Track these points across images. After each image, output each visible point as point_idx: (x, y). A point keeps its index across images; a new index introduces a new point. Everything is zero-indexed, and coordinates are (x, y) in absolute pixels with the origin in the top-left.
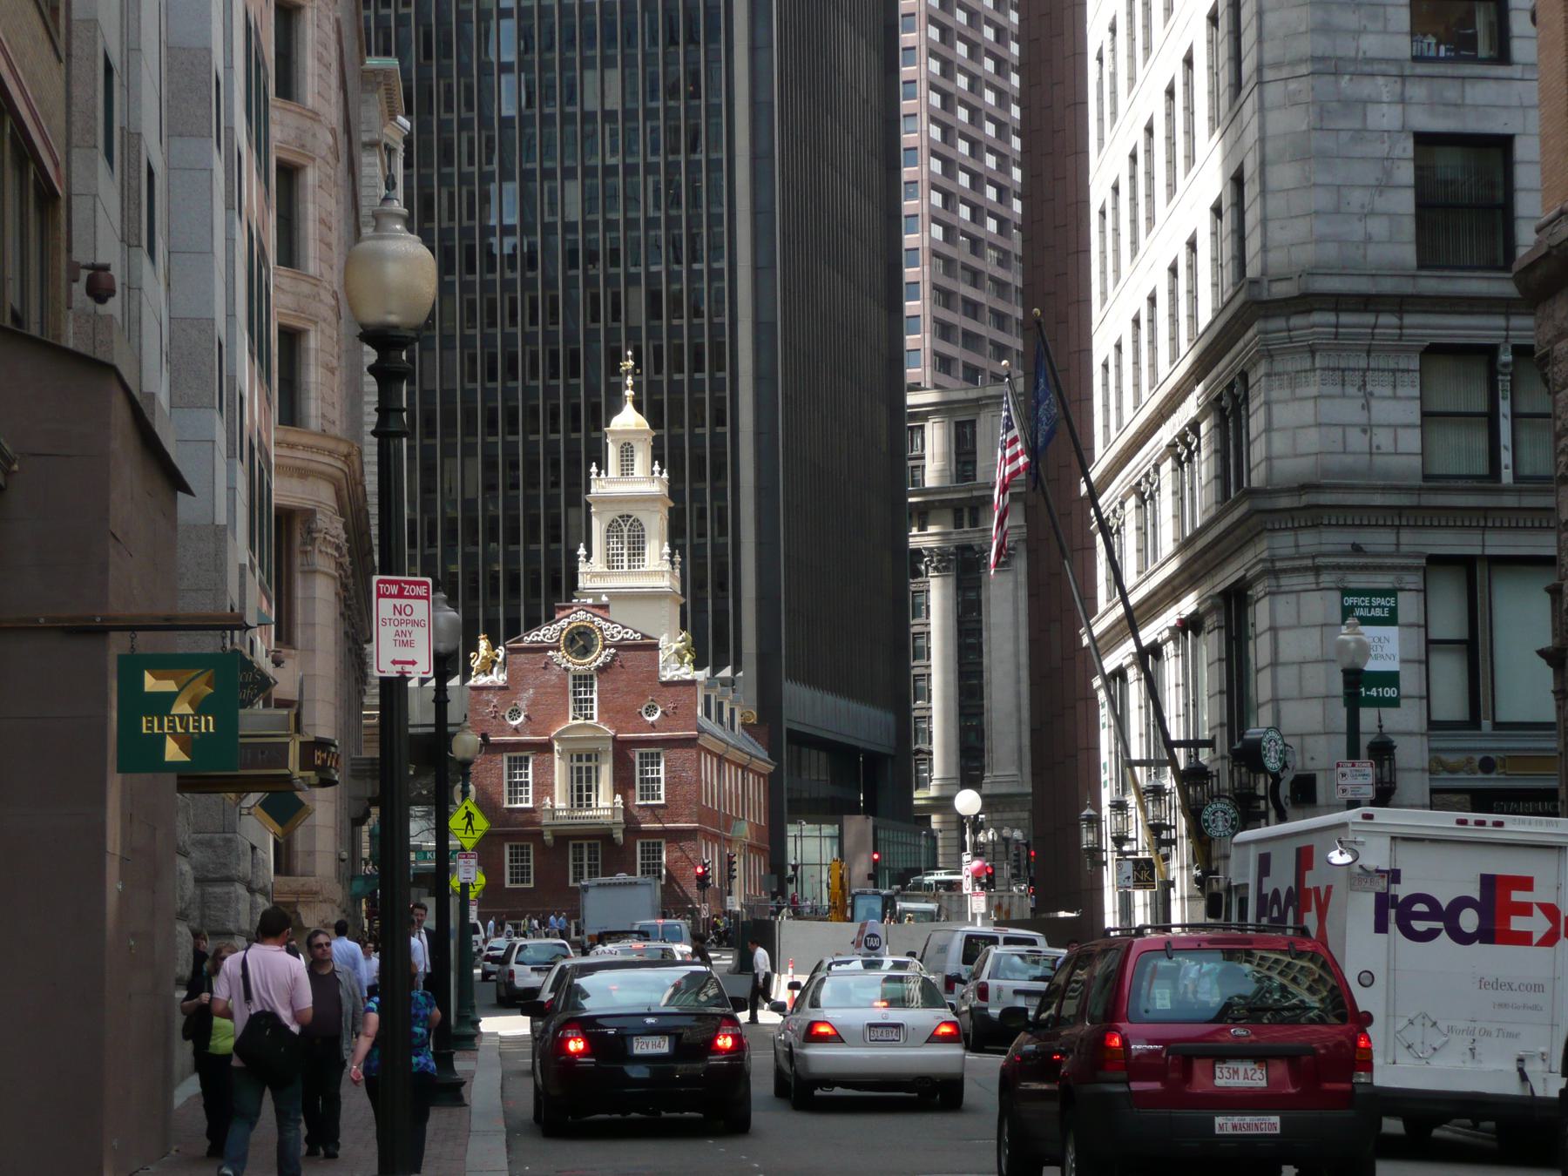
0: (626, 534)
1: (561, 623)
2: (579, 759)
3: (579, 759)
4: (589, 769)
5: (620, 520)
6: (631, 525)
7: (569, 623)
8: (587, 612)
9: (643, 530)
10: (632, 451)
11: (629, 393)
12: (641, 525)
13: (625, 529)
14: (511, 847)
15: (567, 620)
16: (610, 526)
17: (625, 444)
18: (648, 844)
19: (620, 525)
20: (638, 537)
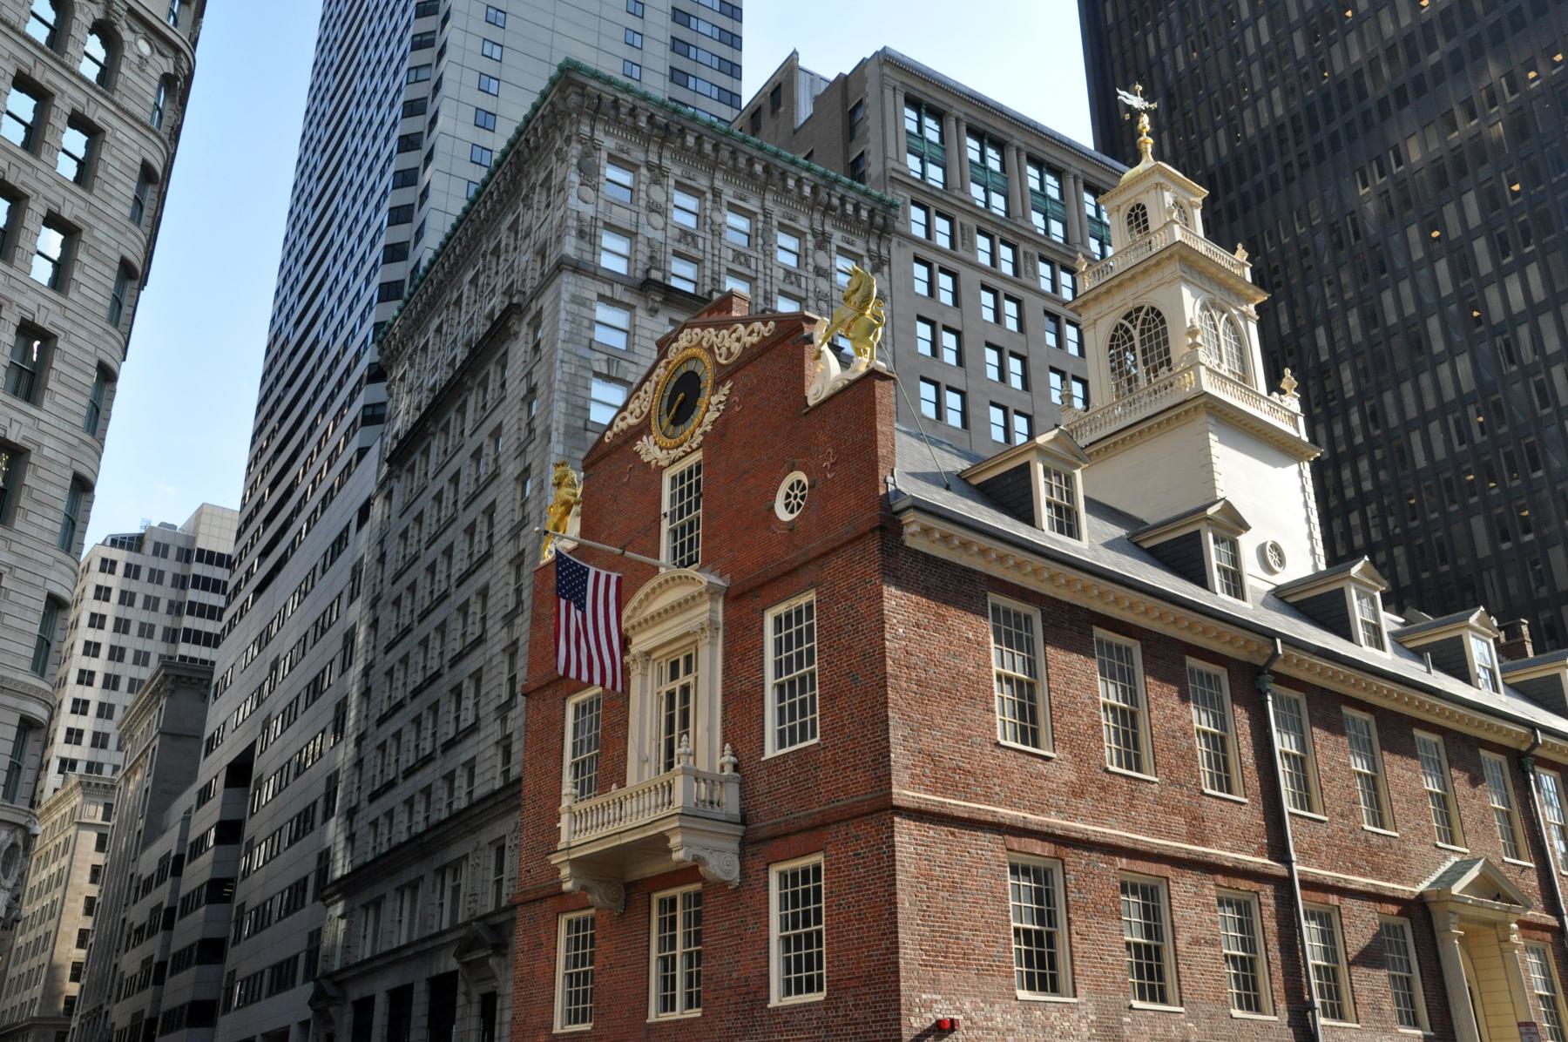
0: (1137, 341)
1: (654, 378)
2: (674, 675)
3: (674, 675)
4: (685, 689)
5: (1126, 323)
6: (1143, 323)
7: (668, 363)
8: (692, 327)
9: (1163, 322)
10: (1144, 214)
11: (1147, 143)
12: (1159, 314)
13: (1136, 333)
14: (574, 926)
15: (663, 363)
16: (1113, 338)
17: (1133, 210)
18: (795, 875)
19: (1127, 331)
20: (1157, 334)
